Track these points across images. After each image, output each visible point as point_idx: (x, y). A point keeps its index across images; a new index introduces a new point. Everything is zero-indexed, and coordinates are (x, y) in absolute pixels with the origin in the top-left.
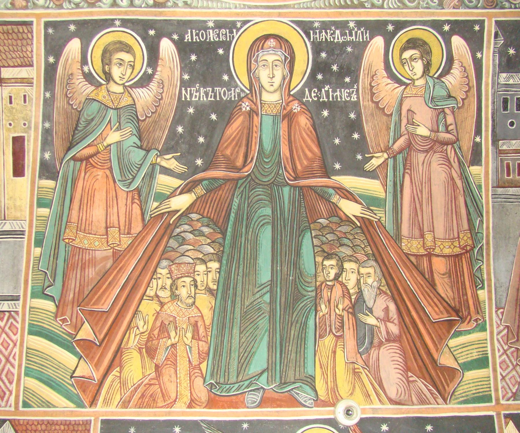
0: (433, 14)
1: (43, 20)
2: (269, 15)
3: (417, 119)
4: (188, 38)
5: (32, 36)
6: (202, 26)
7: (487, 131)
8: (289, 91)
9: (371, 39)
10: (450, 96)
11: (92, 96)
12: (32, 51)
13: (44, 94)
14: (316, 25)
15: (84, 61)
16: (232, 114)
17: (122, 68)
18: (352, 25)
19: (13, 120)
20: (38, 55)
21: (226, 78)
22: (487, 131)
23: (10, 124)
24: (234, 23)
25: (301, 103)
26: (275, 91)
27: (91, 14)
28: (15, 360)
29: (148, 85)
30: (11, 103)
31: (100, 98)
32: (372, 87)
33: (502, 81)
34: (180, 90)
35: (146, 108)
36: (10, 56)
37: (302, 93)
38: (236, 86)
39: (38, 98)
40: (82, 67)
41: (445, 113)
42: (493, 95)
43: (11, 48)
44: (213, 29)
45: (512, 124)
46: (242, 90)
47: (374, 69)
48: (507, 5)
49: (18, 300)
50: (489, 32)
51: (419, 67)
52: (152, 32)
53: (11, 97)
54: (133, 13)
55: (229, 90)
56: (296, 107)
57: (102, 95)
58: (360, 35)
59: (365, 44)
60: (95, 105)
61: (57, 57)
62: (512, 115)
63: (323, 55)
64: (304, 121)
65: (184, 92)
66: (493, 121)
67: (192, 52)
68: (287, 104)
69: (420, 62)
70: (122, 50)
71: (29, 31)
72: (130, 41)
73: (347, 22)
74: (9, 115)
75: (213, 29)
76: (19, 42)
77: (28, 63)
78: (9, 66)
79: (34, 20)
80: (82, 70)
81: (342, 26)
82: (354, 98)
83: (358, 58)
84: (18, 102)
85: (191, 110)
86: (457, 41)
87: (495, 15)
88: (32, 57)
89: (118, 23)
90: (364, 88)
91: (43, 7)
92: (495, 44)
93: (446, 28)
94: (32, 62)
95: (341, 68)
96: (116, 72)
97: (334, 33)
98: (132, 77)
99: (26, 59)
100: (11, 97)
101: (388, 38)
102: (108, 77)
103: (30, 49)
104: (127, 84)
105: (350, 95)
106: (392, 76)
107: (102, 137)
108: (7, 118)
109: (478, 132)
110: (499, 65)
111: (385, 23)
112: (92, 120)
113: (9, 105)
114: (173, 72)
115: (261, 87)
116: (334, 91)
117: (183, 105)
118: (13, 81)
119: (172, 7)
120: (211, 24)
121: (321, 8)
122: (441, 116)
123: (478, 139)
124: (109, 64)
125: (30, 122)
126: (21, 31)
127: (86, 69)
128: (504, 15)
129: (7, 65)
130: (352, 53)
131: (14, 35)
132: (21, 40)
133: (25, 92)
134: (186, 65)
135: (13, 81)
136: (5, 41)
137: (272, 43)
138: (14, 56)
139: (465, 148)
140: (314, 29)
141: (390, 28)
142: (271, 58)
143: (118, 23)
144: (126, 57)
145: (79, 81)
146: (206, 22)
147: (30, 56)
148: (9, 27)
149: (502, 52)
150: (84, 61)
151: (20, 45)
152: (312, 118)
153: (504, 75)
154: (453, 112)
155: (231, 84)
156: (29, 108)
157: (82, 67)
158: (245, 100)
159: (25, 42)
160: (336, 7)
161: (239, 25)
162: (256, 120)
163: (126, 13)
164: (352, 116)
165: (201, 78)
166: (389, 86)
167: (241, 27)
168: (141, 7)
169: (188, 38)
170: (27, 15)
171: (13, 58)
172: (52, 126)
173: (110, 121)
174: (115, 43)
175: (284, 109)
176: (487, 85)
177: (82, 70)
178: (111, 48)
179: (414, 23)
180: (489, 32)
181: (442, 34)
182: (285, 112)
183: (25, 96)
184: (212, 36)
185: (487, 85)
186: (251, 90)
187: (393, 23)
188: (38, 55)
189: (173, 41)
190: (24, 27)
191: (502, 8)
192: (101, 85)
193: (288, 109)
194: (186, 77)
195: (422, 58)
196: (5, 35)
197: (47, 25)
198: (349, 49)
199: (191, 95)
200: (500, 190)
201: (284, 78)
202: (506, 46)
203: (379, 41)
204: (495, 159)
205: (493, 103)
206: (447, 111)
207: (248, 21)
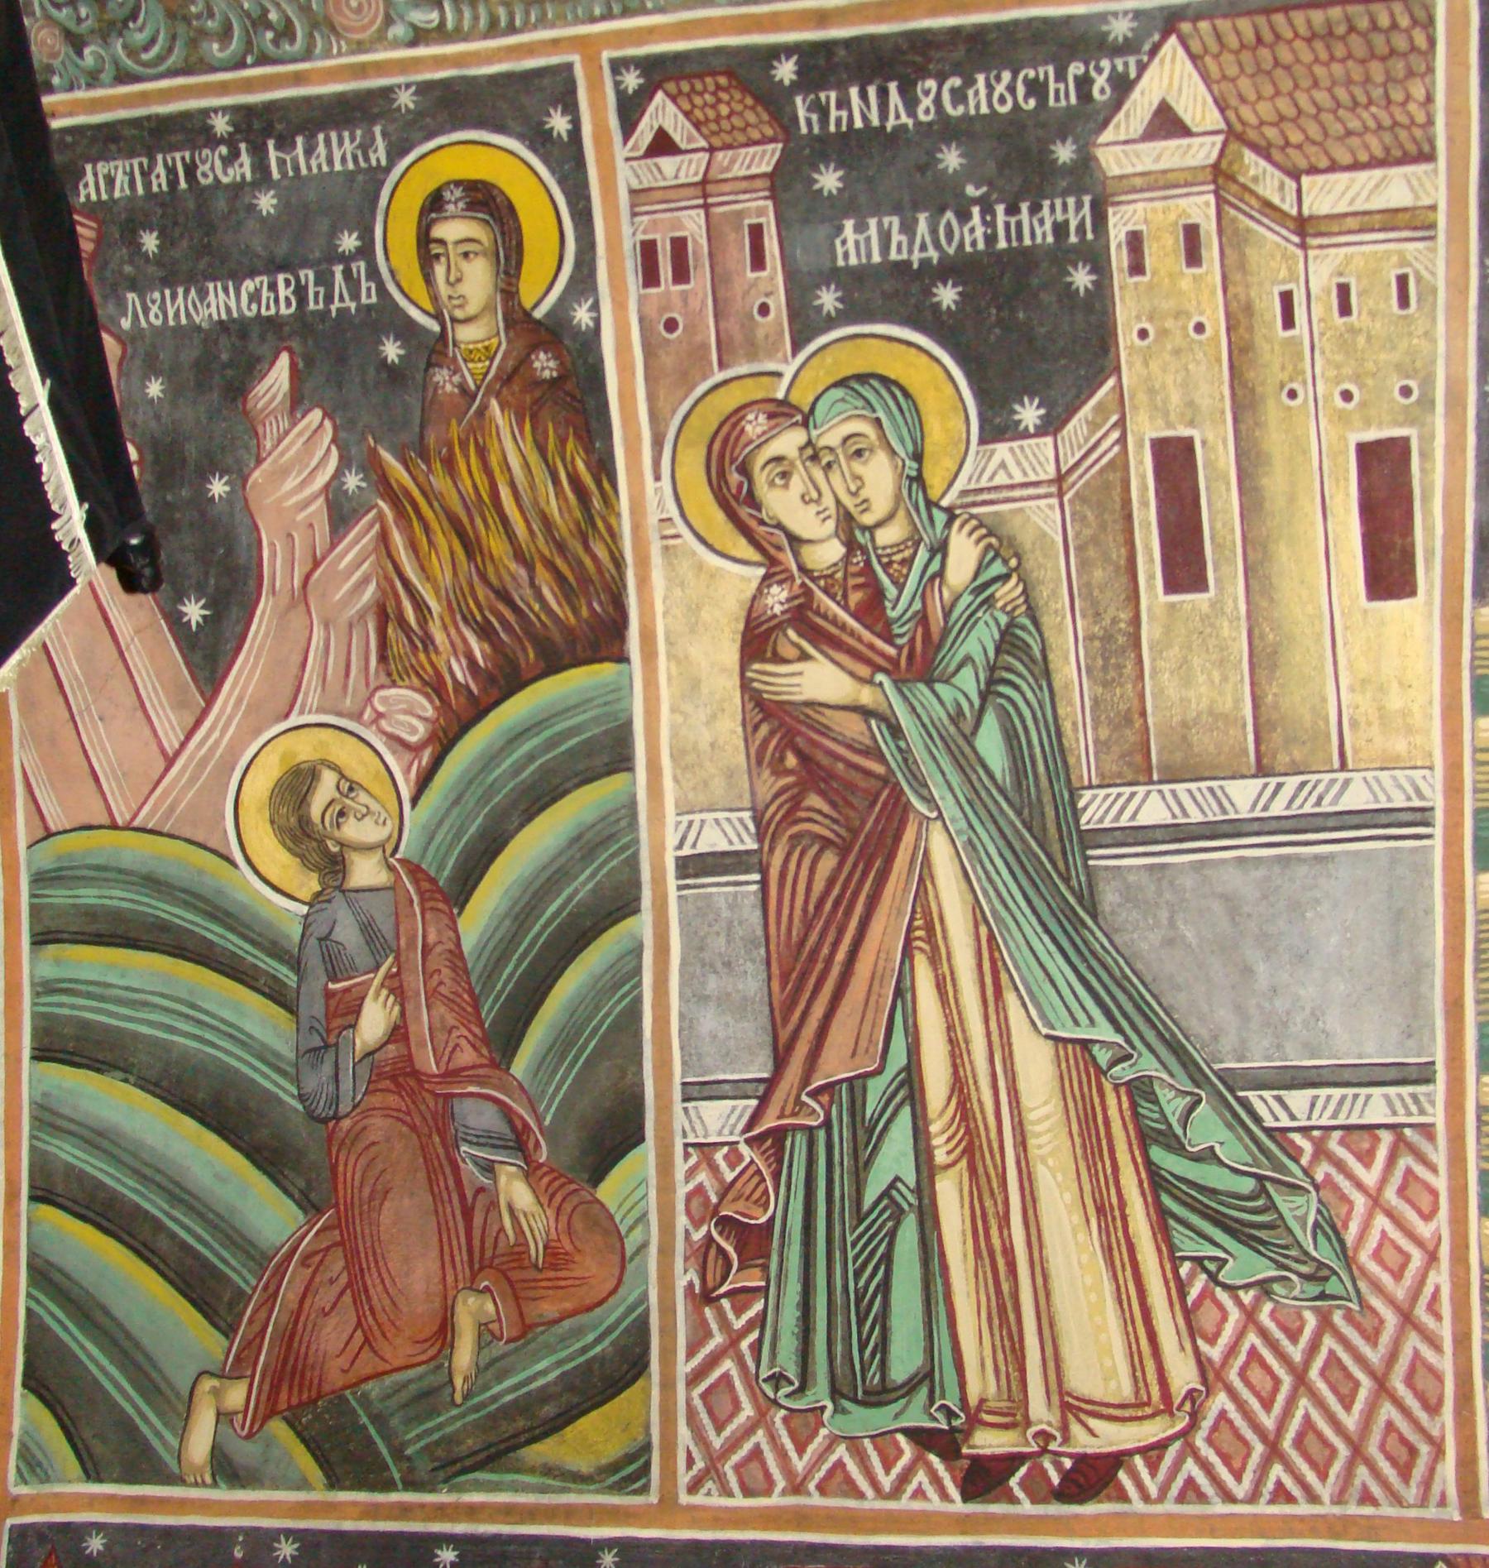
5: (1432, 42)
12: (1429, 99)
19: (1357, 378)
23: (1347, 396)
28: (1438, 1317)
30: (1345, 309)
36: (1336, 129)
43: (1341, 94)
49: (1429, 1080)
53: (1344, 291)
71: (1415, 22)
74: (1339, 358)
76: (1377, 70)
77: (1412, 149)
78: (1334, 167)
88: (1430, 122)
94: (1431, 142)
99: (1403, 135)
100: (1344, 291)
103: (1418, 92)
108: (1332, 373)
113: (1340, 321)
118: (1351, 223)
125: (1428, 382)
126: (1384, 21)
129: (1324, 163)
131: (1355, 41)
132: (1383, 59)
133: (1403, 262)
135: (1351, 223)
136: (1319, 71)
138: (1354, 124)
147: (1421, 118)
151: (1379, 78)
156: (1421, 326)
159: (1398, 67)
171: (1349, 133)
183: (1402, 281)
196: (1319, 46)
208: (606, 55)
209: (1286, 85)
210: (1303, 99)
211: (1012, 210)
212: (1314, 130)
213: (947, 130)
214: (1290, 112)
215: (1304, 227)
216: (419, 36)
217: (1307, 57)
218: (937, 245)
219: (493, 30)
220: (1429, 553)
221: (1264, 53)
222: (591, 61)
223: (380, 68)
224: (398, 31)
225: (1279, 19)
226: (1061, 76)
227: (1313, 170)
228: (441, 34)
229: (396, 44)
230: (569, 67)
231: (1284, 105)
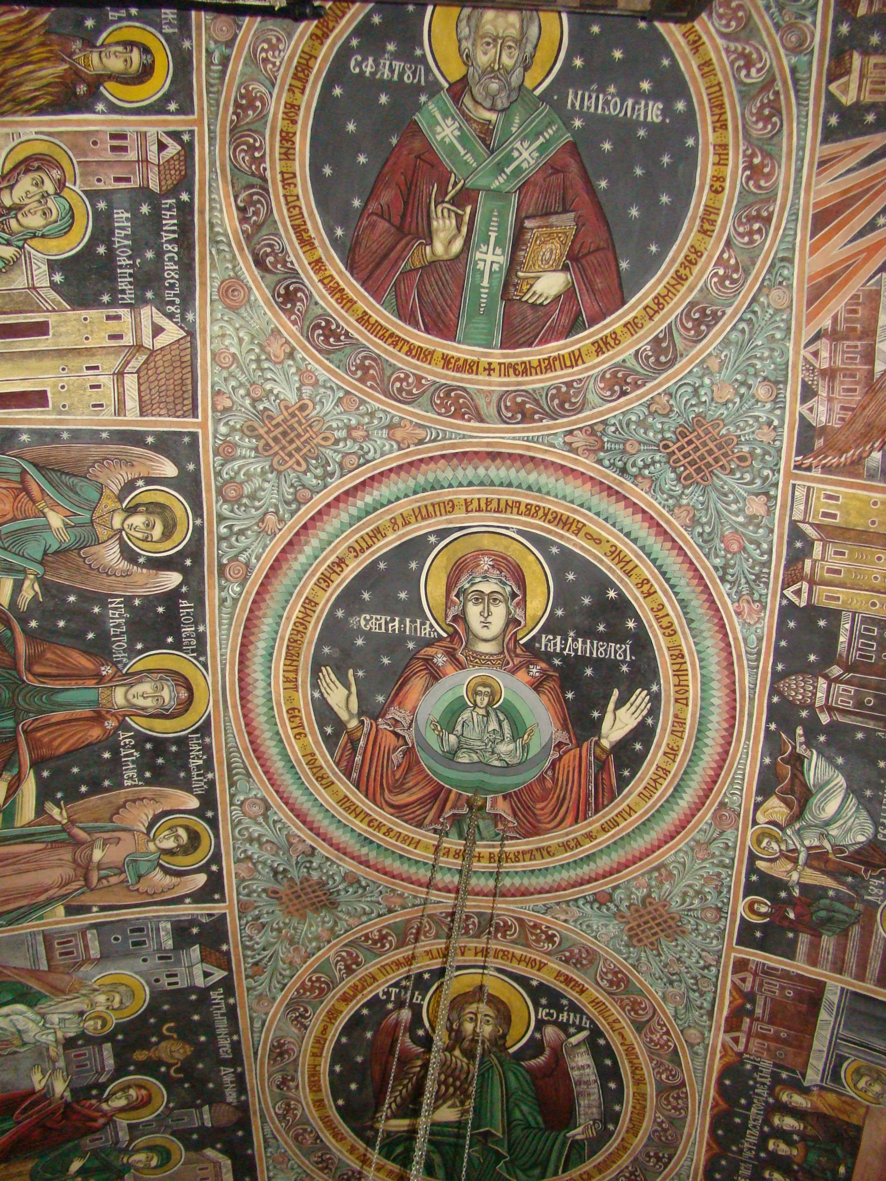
0: (228, 854)
1: (200, 431)
2: (215, 691)
3: (112, 849)
4: (184, 603)
6: (199, 618)
7: (105, 916)
8: (129, 716)
9: (196, 796)
10: (140, 877)
11: (106, 492)
12: (160, 415)
13: (105, 431)
14: (207, 740)
15: (150, 481)
16: (96, 655)
17: (142, 526)
18: (210, 776)
19: (68, 391)
20: (156, 423)
21: (139, 646)
22: (105, 916)
23: (63, 387)
24: (204, 653)
25: (117, 729)
26: (127, 700)
27: (209, 491)
29: (124, 558)
30: (92, 387)
31: (104, 501)
32: (142, 799)
33: (162, 925)
34: (121, 596)
35: (95, 557)
36: (152, 386)
37: (129, 728)
38: (130, 659)
39: (99, 423)
40: (142, 478)
41: (120, 874)
42: (146, 918)
43: (164, 388)
44: (196, 631)
45: (116, 939)
46: (125, 665)
47: (162, 800)
48: (244, 922)
50: (214, 908)
51: (170, 844)
52: (188, 562)
53: (98, 387)
54: (211, 540)
55: (124, 651)
56: (110, 724)
57: (108, 503)
58: (199, 785)
59: (190, 790)
60: (95, 496)
61: (154, 448)
62: (125, 939)
63: (174, 749)
64: (95, 733)
65: (118, 600)
66: (118, 921)
67: (167, 609)
68: (113, 715)
69: (175, 845)
70: (165, 527)
72: (177, 537)
73: (213, 771)
75: (196, 631)
76: (171, 399)
78: (139, 384)
79: (199, 420)
80: (138, 479)
81: (208, 766)
82: (127, 783)
83: (174, 783)
84: (94, 396)
85: (96, 610)
86: (201, 879)
87: (232, 912)
89: (198, 522)
90: (140, 791)
91: (216, 431)
92: (202, 915)
93: (214, 868)
95: (161, 767)
96: (138, 520)
97: (199, 759)
98: (133, 539)
100: (98, 387)
101: (198, 813)
102: (132, 511)
103: (162, 412)
104: (124, 533)
105: (131, 778)
106: (156, 818)
107: (54, 507)
109: (103, 909)
110: (180, 921)
111: (215, 809)
112: (76, 493)
114: (141, 587)
115: (131, 685)
116: (133, 762)
117: (103, 599)
118: (121, 390)
119: (220, 585)
120: (201, 629)
121: (227, 744)
122: (116, 871)
123: (95, 909)
124: (148, 512)
125: (68, 413)
126: (186, 402)
127: (140, 483)
128: (233, 920)
130: (179, 779)
131: (179, 393)
133: (107, 406)
134: (150, 601)
135: (121, 390)
137: (184, 694)
138: (153, 392)
139: (83, 898)
140: (202, 737)
141: (210, 814)
142: (166, 694)
143: (198, 522)
144: (157, 532)
145: (124, 475)
146: (204, 622)
148: (190, 387)
149: (193, 921)
150: (150, 481)
152: (99, 742)
153: (169, 926)
154: (122, 882)
155: (132, 652)
156: (86, 411)
157: (142, 478)
158: (115, 669)
159: (171, 406)
160: (228, 759)
161: (202, 659)
162: (91, 683)
163: (211, 532)
164: (107, 783)
165: (137, 619)
166: (145, 817)
167: (199, 662)
168: (218, 549)
169: (184, 603)
170: (205, 411)
172: (64, 442)
173: (75, 514)
174: (174, 519)
175: (108, 712)
176: (157, 911)
177: (138, 479)
178: (168, 514)
179: (217, 836)
180: (214, 908)
181: (208, 864)
182: (104, 713)
183: (101, 405)
184: (188, 630)
185: (157, 911)
186: (127, 674)
187: (215, 818)
188: (156, 423)
189: (180, 586)
190: (190, 407)
191: (240, 918)
192: (121, 502)
193: (108, 716)
194: (137, 602)
195: (179, 846)
197: (194, 436)
198: (182, 774)
199: (115, 609)
200: (40, 938)
201: (143, 709)
202: (201, 925)
203: (194, 803)
204: (75, 928)
205: (138, 919)
206: (123, 876)
207: (207, 670)
208: (196, 129)
209: (167, 371)
210: (163, 375)
211: (131, 275)
212: (152, 379)
213: (160, 254)
214: (159, 371)
215: (120, 374)
216: (209, 53)
217: (176, 377)
218: (120, 247)
219: (209, 84)
220: (9, 414)
221: (178, 364)
222: (194, 123)
223: (199, 35)
224: (212, 45)
225: (189, 369)
226: (175, 296)
227: (139, 378)
228: (209, 64)
229: (207, 43)
230: (193, 113)
231: (161, 369)
